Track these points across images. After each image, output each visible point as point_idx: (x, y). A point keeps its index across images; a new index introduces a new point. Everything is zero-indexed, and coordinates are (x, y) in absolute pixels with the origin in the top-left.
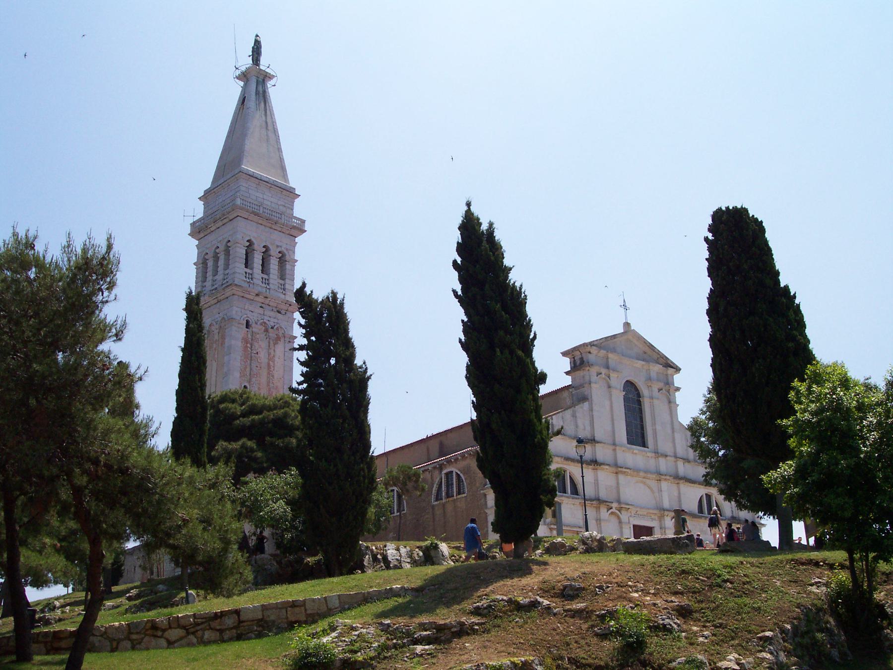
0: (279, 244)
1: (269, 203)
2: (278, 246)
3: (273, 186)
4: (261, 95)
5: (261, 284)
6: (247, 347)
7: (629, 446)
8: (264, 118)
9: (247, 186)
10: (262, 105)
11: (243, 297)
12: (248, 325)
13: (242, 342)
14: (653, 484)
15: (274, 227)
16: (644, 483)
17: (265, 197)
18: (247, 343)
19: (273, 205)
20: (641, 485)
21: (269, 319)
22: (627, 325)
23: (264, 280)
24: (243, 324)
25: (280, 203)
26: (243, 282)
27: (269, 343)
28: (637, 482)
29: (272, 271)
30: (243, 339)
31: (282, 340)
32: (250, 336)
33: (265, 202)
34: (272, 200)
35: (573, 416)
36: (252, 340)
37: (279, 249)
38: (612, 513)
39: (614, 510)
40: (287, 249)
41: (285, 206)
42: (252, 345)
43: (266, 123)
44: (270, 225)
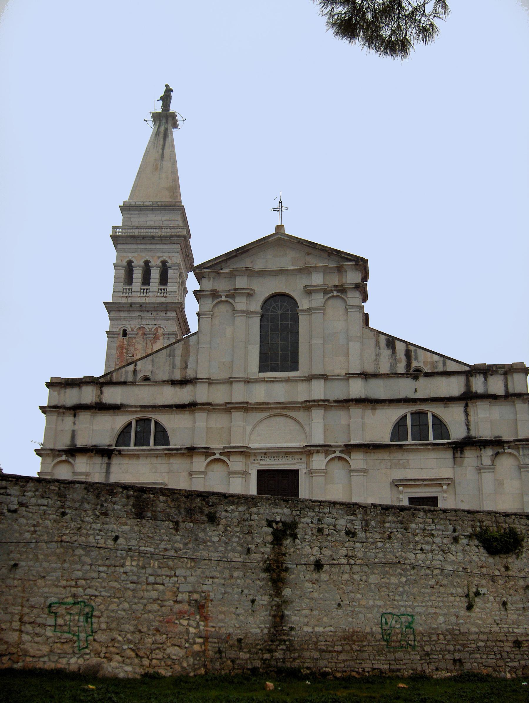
0: (159, 254)
1: (152, 223)
2: (159, 258)
3: (154, 208)
4: (162, 135)
5: (138, 294)
6: (123, 352)
7: (262, 375)
8: (160, 151)
9: (129, 216)
10: (161, 142)
11: (119, 311)
12: (125, 333)
13: (117, 349)
14: (300, 415)
15: (153, 242)
16: (286, 416)
17: (148, 219)
18: (122, 350)
19: (157, 223)
20: (282, 419)
21: (147, 323)
22: (280, 228)
23: (145, 291)
24: (118, 334)
25: (164, 219)
26: (121, 298)
27: (147, 343)
28: (270, 416)
29: (151, 280)
30: (119, 346)
31: (161, 338)
32: (126, 343)
33: (148, 223)
34: (155, 219)
35: (170, 356)
36: (128, 345)
37: (161, 259)
38: (219, 460)
39: (217, 456)
40: (169, 257)
41: (169, 220)
42: (127, 350)
43: (163, 155)
44: (149, 242)
